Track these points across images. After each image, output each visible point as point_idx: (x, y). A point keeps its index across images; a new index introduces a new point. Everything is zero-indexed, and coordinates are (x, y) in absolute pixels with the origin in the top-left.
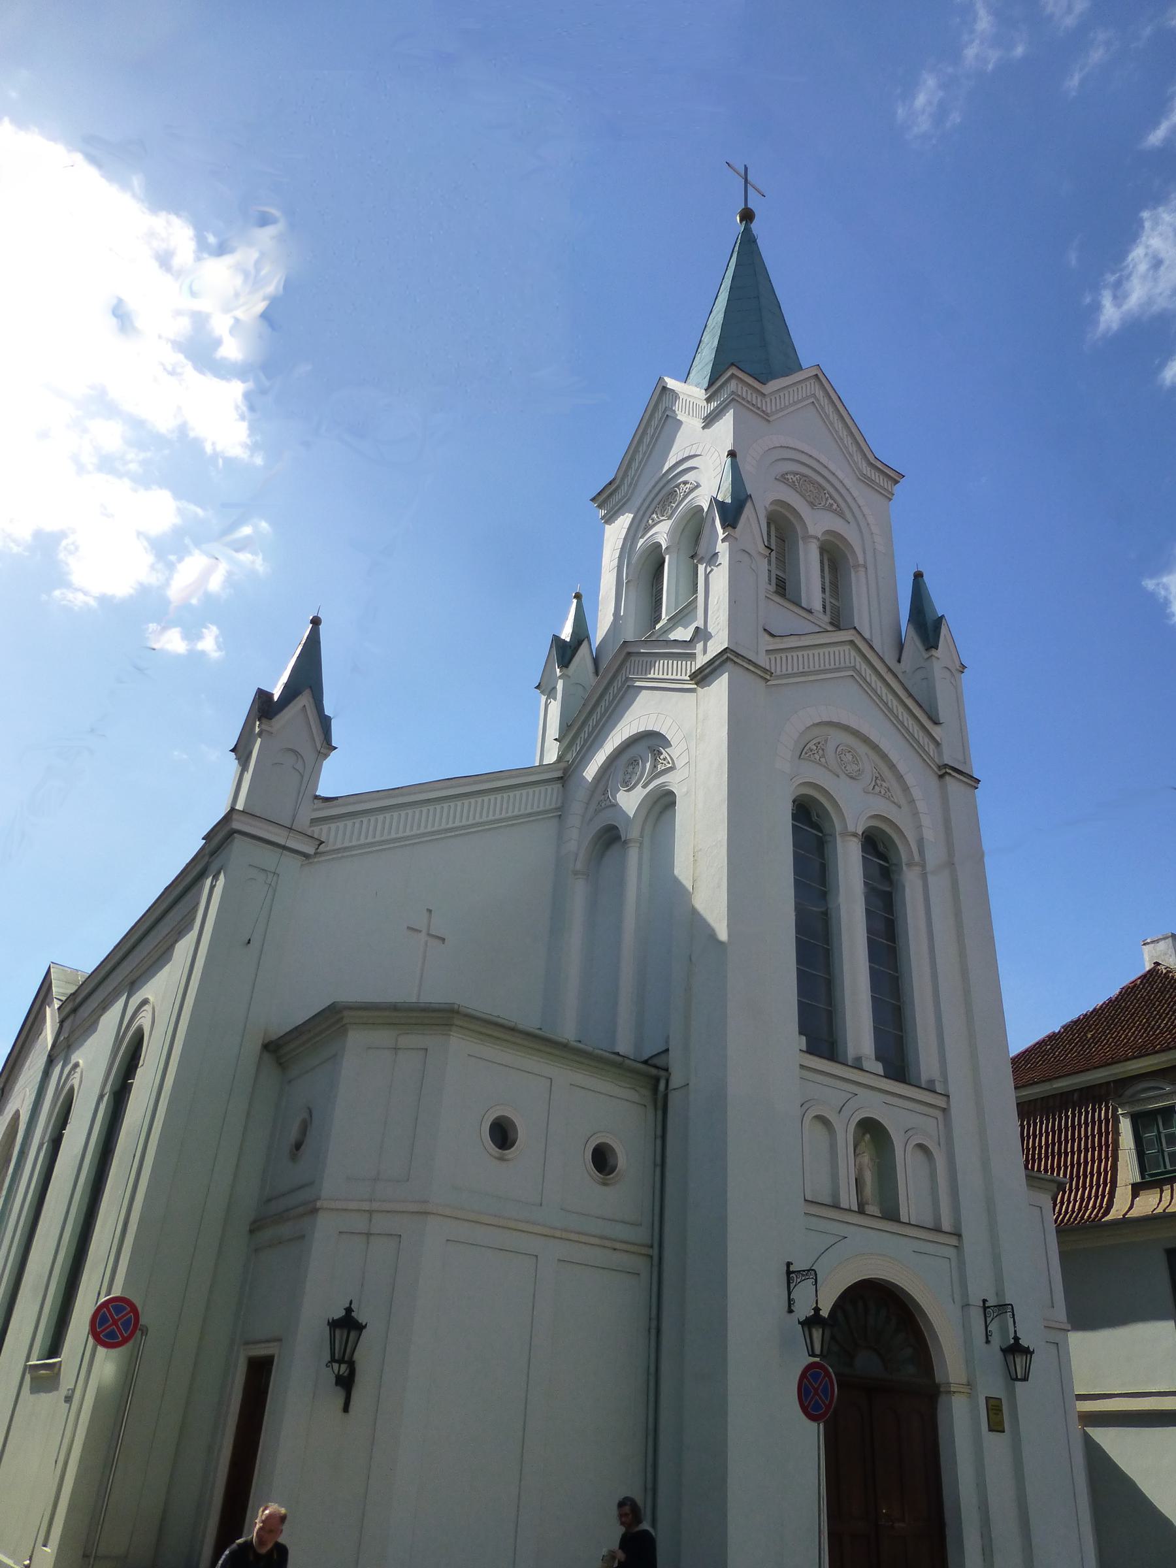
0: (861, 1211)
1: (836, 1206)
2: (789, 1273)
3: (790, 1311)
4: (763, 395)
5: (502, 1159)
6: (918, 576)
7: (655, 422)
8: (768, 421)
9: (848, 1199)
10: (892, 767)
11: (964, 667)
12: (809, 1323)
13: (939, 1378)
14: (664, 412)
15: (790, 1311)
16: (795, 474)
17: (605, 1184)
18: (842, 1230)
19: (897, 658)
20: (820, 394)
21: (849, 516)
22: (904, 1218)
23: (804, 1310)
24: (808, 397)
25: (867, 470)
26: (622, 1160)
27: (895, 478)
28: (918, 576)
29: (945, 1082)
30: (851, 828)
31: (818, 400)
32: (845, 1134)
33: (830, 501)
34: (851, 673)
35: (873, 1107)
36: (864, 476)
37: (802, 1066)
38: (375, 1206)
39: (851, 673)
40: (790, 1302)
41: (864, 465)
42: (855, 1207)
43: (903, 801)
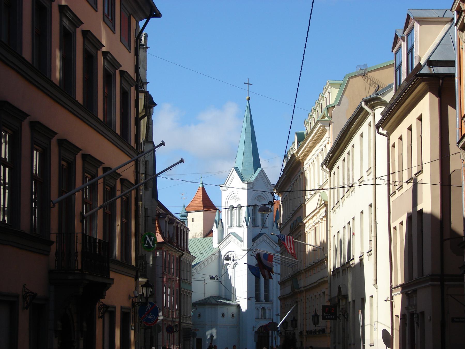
0: (261, 319)
1: (259, 319)
2: (253, 327)
3: (253, 331)
5: (223, 318)
9: (260, 317)
12: (255, 332)
15: (253, 331)
18: (259, 321)
22: (266, 318)
23: (255, 331)
32: (260, 309)
36: (270, 189)
37: (255, 303)
38: (212, 324)
40: (253, 330)
42: (261, 318)
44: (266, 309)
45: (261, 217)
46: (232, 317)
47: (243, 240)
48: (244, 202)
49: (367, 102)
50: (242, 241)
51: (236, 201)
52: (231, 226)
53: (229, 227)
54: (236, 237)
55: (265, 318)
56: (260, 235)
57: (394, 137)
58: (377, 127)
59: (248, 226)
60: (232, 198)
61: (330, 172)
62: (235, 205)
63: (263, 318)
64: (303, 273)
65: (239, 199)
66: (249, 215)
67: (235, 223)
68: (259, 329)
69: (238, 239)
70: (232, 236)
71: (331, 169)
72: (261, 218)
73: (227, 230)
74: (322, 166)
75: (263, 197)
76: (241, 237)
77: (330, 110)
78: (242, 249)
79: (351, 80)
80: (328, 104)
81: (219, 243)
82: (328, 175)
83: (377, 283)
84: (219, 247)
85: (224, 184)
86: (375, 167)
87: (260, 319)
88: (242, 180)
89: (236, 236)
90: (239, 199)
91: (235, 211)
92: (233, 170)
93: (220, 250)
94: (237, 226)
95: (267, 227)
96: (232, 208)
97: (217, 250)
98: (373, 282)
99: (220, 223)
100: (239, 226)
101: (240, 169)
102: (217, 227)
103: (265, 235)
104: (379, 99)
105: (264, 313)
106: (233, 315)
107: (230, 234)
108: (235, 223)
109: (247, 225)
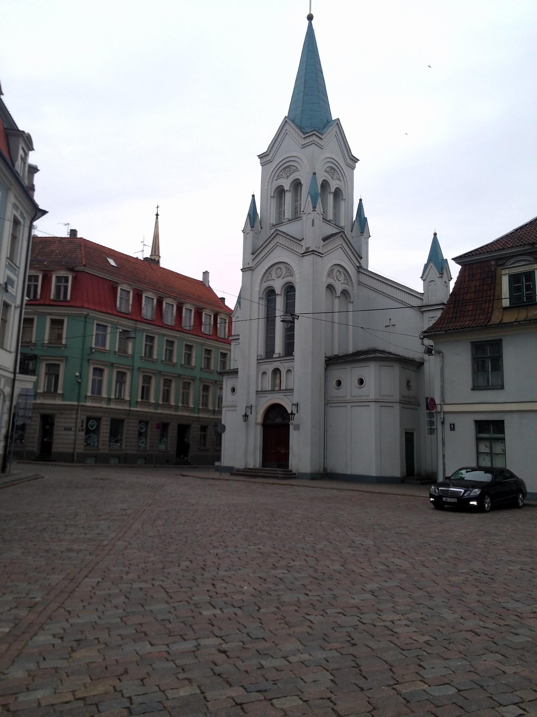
4: (321, 139)
6: (361, 200)
7: (282, 134)
8: (323, 149)
11: (370, 236)
14: (286, 131)
16: (328, 167)
20: (338, 131)
21: (342, 179)
24: (334, 134)
25: (349, 161)
27: (356, 160)
28: (361, 200)
30: (338, 295)
31: (337, 133)
33: (337, 175)
34: (341, 246)
39: (341, 246)
43: (350, 284)
60: (281, 173)
65: (297, 170)
78: (302, 254)
90: (297, 170)
103: (342, 236)
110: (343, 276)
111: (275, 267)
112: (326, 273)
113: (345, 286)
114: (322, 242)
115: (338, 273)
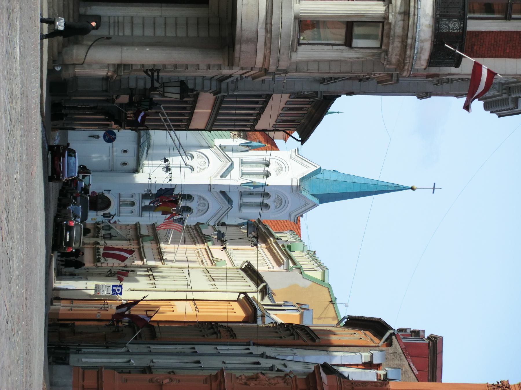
0: (120, 201)
4: (297, 192)
5: (121, 152)
9: (122, 199)
10: (205, 213)
12: (102, 193)
13: (99, 211)
17: (121, 164)
19: (241, 217)
23: (104, 192)
26: (125, 166)
29: (144, 216)
31: (308, 205)
32: (131, 199)
35: (137, 204)
36: (291, 215)
41: (295, 215)
42: (120, 200)
44: (131, 208)
45: (255, 203)
46: (122, 163)
47: (223, 179)
48: (271, 181)
49: (265, 287)
50: (222, 177)
51: (276, 170)
52: (242, 163)
53: (242, 160)
54: (227, 169)
55: (120, 206)
56: (230, 201)
57: (236, 305)
58: (244, 293)
59: (241, 185)
60: (279, 165)
61: (241, 269)
62: (271, 169)
63: (121, 203)
64: (157, 246)
65: (277, 174)
66: (255, 187)
67: (247, 169)
68: (107, 197)
69: (224, 172)
70: (230, 164)
71: (244, 270)
72: (253, 203)
73: (237, 157)
74: (247, 262)
75: (280, 206)
76: (227, 176)
77: (298, 270)
78: (210, 177)
79: (327, 289)
80: (304, 269)
81: (220, 146)
82: (239, 267)
83: (131, 291)
84: (215, 147)
85: (298, 154)
86: (216, 292)
87: (120, 199)
88: (302, 180)
89: (230, 168)
90: (277, 174)
91: (261, 169)
92: (317, 167)
93: (211, 147)
94: (242, 170)
95: (240, 210)
96: (267, 164)
97: (211, 144)
98: (132, 289)
99: (246, 149)
100: (242, 174)
101: (319, 176)
102: (241, 145)
104: (266, 295)
105: (126, 205)
106: (125, 164)
107: (232, 161)
108: (247, 169)
109: (242, 184)
110: (202, 208)
111: (207, 161)
112: (199, 194)
113: (195, 211)
114: (219, 191)
115: (204, 205)
